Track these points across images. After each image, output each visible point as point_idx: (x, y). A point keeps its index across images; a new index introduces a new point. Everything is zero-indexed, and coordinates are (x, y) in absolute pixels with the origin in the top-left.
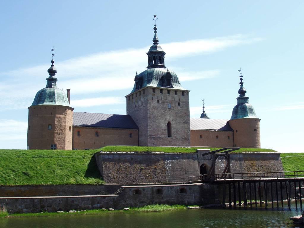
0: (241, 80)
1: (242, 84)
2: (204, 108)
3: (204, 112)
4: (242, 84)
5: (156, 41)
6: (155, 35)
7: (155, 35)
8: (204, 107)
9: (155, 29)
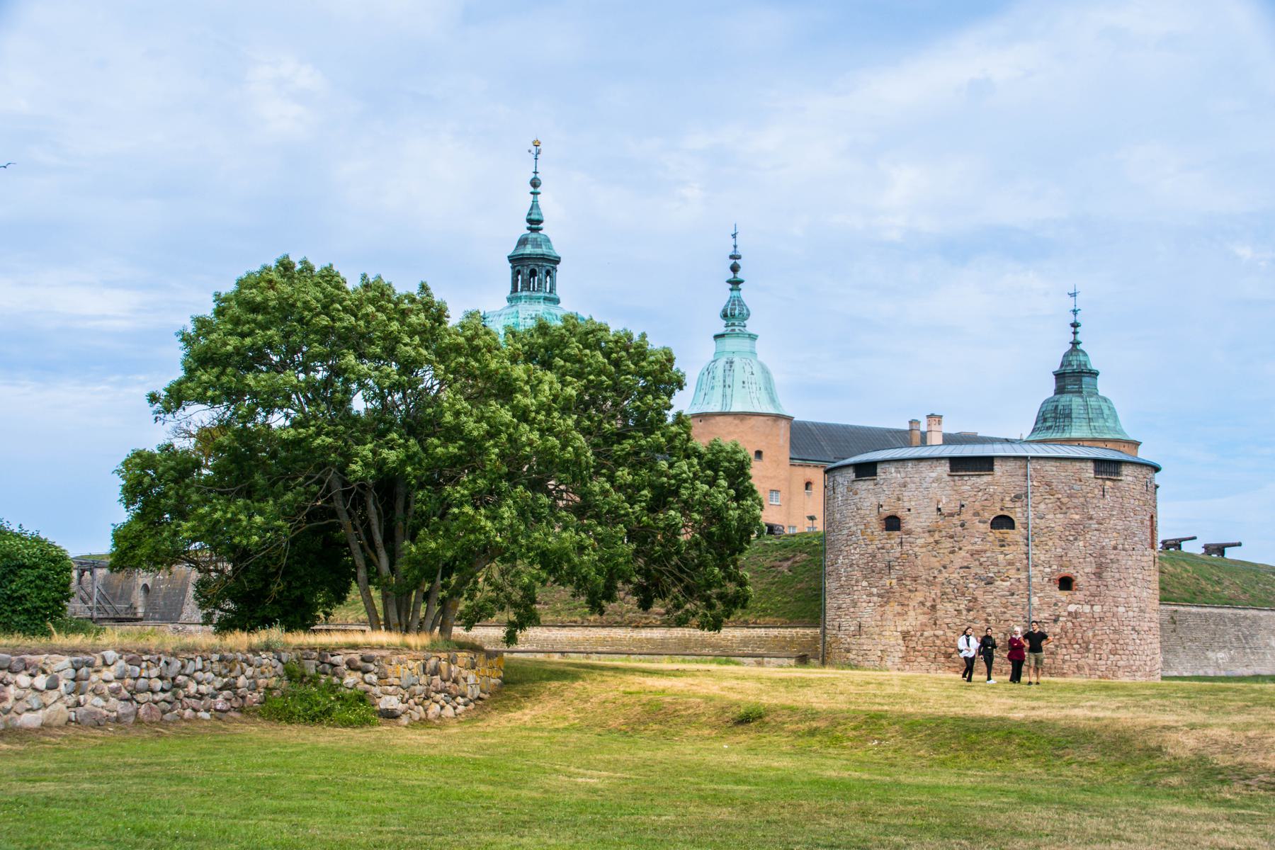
0: (735, 269)
1: (735, 283)
2: (1078, 329)
3: (1075, 344)
4: (735, 283)
5: (534, 223)
6: (535, 206)
7: (535, 206)
8: (1075, 325)
9: (535, 183)
